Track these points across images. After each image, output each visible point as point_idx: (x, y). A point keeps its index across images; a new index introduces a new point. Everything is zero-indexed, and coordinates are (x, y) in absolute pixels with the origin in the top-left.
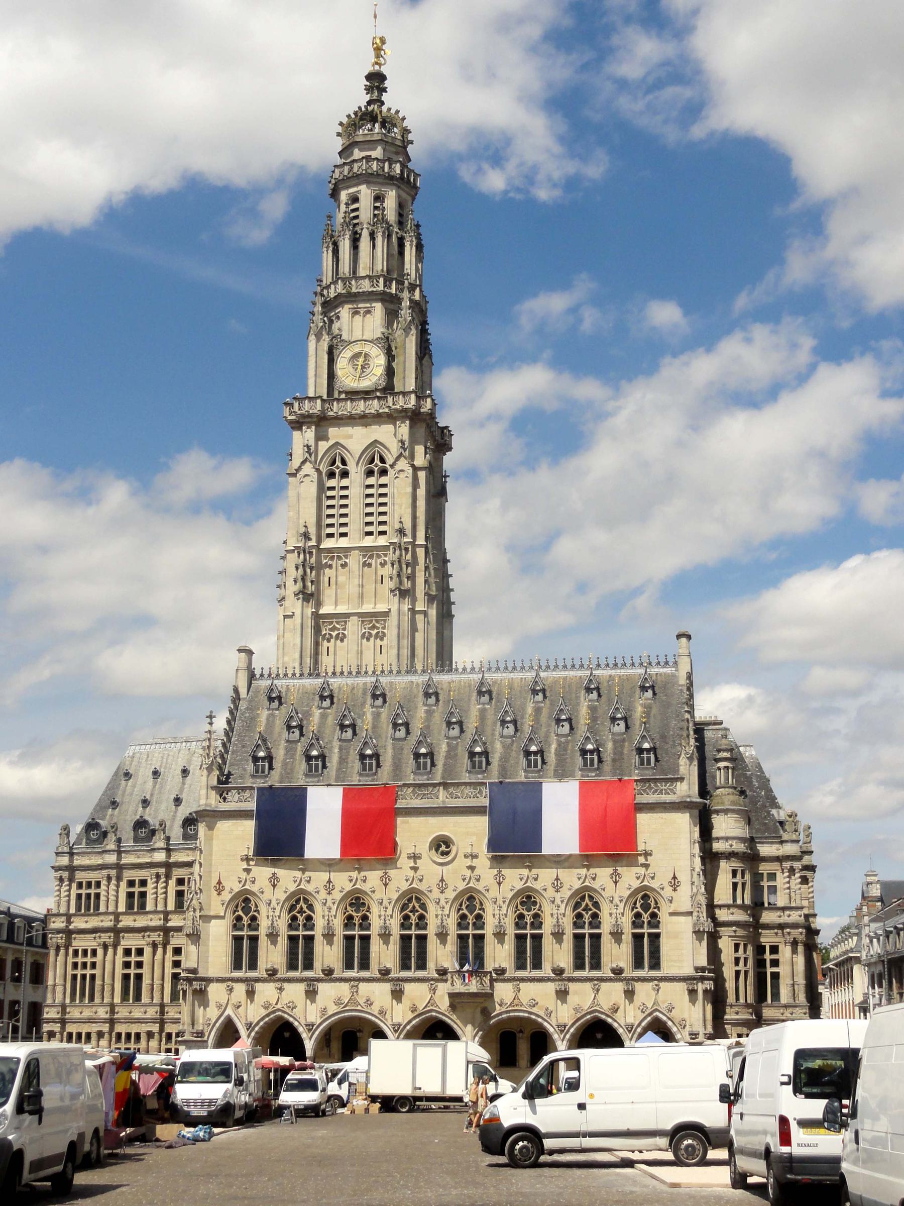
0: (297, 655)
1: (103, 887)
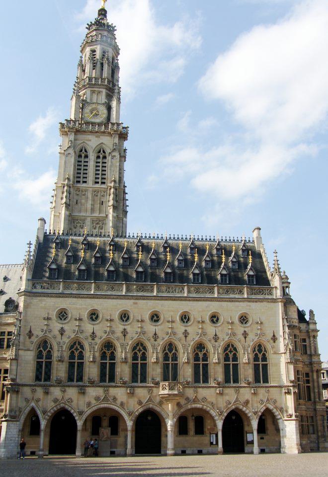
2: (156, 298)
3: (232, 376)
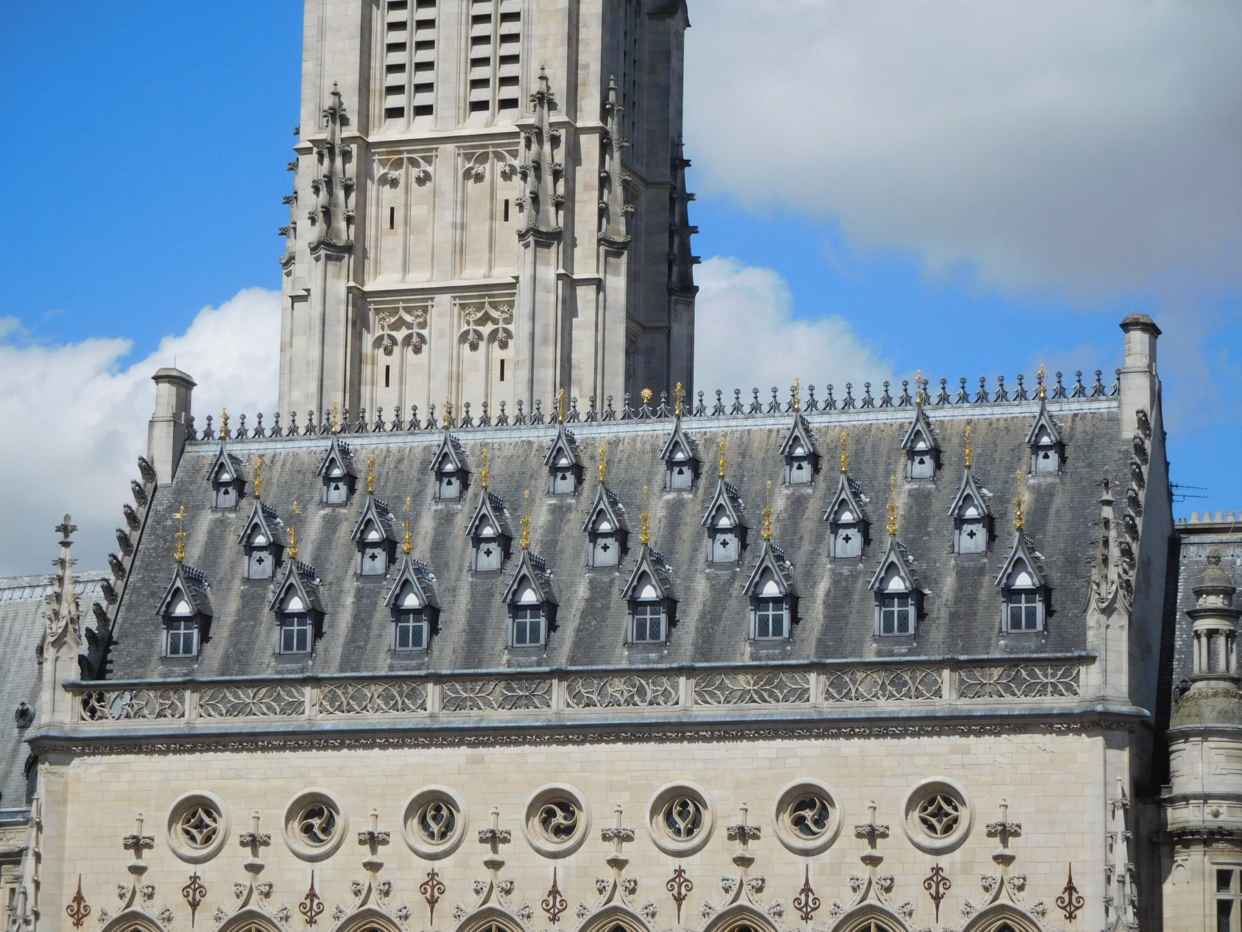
0: (313, 387)
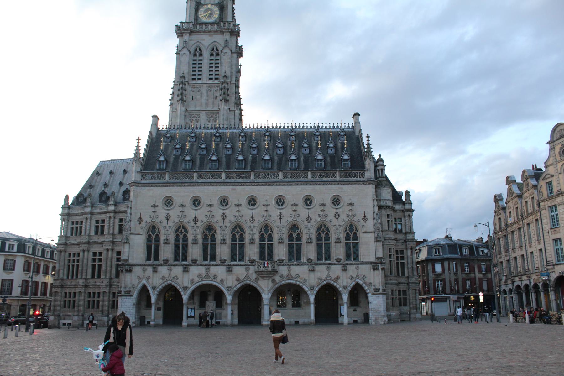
1: (84, 223)
2: (253, 183)
3: (324, 255)
